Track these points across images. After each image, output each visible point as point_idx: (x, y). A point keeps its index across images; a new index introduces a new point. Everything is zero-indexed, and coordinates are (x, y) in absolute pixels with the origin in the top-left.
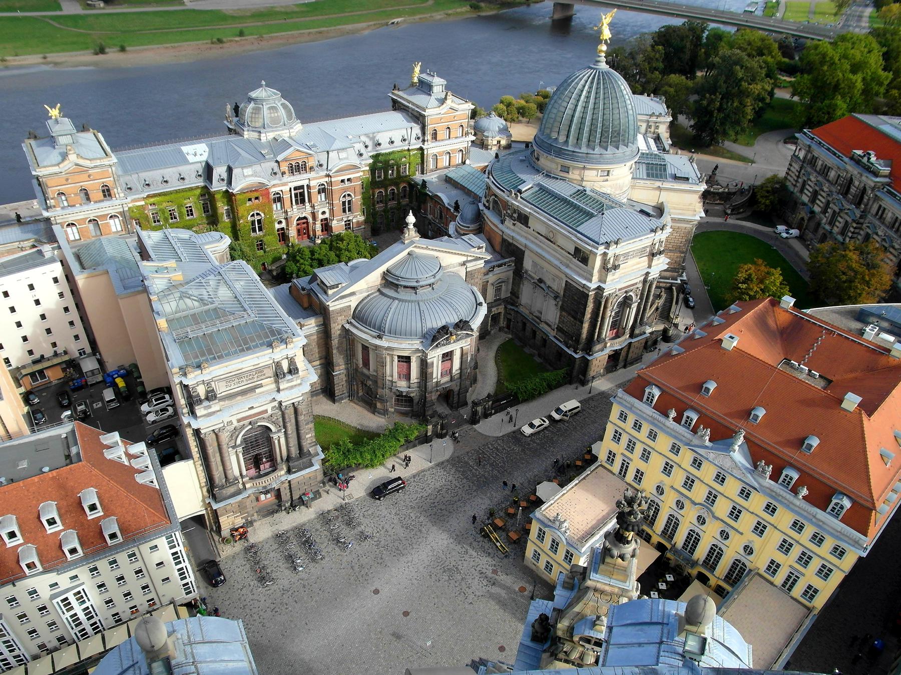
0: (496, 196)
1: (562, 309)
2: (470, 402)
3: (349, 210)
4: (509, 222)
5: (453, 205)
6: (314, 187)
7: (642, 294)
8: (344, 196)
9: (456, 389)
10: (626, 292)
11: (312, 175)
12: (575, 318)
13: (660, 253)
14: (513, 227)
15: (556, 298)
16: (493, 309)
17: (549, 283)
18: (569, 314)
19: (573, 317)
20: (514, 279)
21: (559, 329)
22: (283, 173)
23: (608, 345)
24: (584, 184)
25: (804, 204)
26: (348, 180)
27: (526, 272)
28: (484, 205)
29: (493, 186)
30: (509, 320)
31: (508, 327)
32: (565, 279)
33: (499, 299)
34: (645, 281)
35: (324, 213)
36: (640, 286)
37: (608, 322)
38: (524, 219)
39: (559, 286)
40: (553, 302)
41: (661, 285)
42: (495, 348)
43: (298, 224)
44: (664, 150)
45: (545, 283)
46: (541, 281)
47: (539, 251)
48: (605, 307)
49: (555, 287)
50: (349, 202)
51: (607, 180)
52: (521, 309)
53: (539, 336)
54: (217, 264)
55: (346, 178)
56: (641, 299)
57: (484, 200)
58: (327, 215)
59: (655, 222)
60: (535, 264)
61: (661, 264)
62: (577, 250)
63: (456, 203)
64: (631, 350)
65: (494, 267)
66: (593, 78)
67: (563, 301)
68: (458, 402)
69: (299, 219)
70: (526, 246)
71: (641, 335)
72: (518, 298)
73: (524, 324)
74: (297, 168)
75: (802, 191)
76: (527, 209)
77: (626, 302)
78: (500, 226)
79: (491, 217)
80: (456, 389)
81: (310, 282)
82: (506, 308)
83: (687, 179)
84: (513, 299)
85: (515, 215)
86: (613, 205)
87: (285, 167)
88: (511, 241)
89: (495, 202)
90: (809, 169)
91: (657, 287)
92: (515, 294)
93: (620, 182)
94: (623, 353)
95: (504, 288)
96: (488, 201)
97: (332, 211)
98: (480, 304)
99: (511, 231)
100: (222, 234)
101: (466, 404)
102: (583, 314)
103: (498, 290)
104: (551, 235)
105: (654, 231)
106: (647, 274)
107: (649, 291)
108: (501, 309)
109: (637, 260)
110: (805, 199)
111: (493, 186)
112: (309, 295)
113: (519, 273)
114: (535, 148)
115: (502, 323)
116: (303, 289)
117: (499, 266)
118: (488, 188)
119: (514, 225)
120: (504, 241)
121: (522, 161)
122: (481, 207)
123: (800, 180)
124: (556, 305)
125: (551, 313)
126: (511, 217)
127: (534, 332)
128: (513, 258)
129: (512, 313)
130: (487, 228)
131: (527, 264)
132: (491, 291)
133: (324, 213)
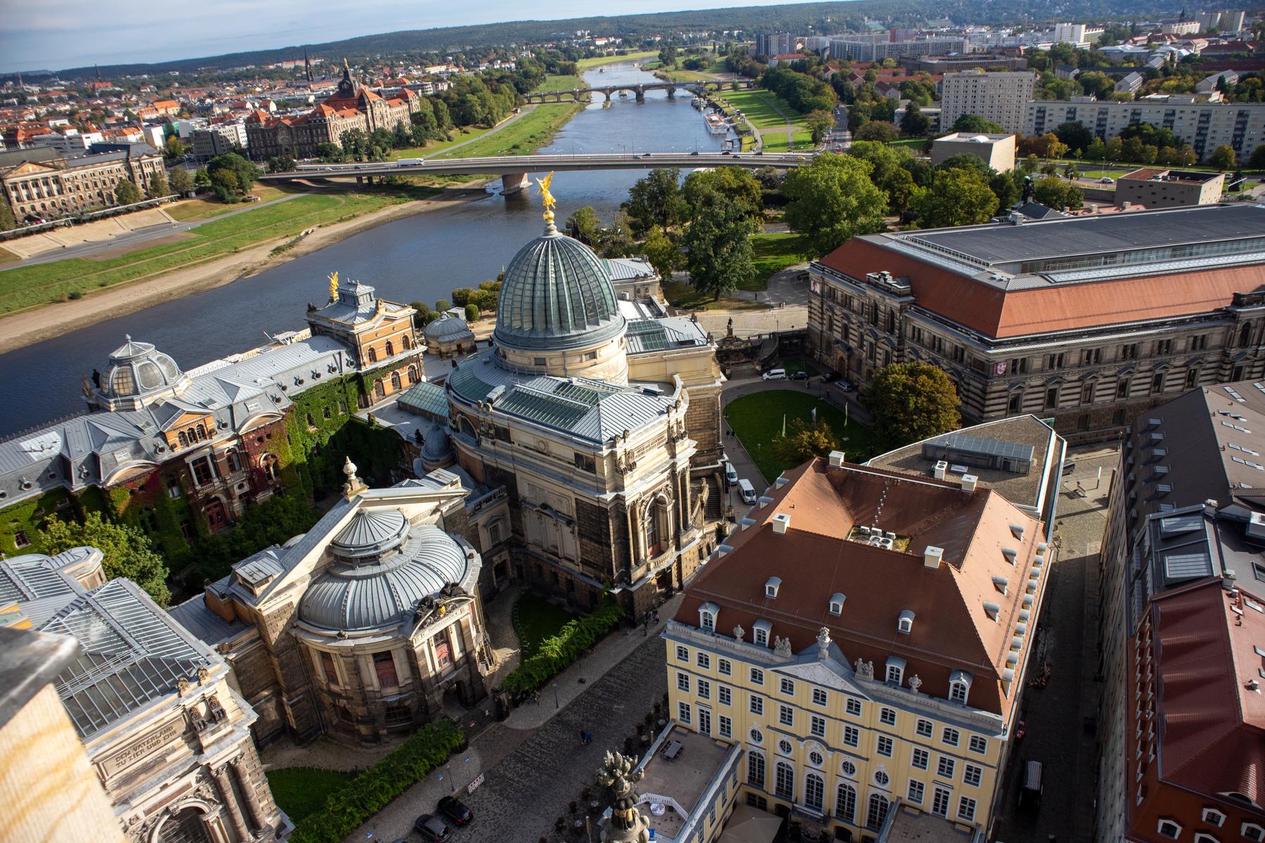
1: (581, 535)
2: (489, 691)
4: (486, 444)
7: (676, 491)
9: (466, 678)
10: (654, 494)
12: (600, 543)
13: (682, 436)
14: (492, 447)
15: (569, 522)
16: (495, 559)
17: (555, 507)
18: (591, 539)
19: (597, 542)
20: (511, 513)
21: (585, 562)
23: (652, 566)
25: (837, 342)
27: (524, 500)
29: (454, 402)
30: (519, 568)
31: (521, 576)
32: (574, 497)
33: (499, 544)
34: (673, 475)
37: (643, 537)
38: (503, 434)
39: (568, 508)
40: (567, 530)
42: (509, 609)
45: (551, 508)
46: (545, 506)
48: (634, 520)
49: (565, 511)
52: (532, 548)
53: (562, 577)
56: (676, 497)
59: (665, 401)
60: (532, 487)
61: (686, 449)
62: (578, 457)
64: (683, 566)
65: (480, 504)
66: (547, 250)
67: (579, 526)
68: (474, 696)
71: (690, 542)
72: (523, 535)
73: (540, 567)
75: (831, 329)
77: (656, 507)
80: (466, 678)
81: (230, 584)
82: (510, 552)
84: (516, 542)
85: (492, 432)
89: (464, 421)
91: (692, 480)
92: (518, 531)
94: (674, 572)
95: (500, 527)
96: (454, 422)
100: (90, 548)
101: (486, 694)
103: (494, 532)
104: (542, 446)
106: (674, 465)
107: (684, 486)
108: (505, 555)
109: (655, 451)
110: (838, 336)
111: (454, 402)
112: (232, 603)
113: (516, 504)
115: (512, 573)
116: (223, 596)
117: (487, 500)
118: (451, 405)
119: (494, 444)
120: (486, 467)
121: (486, 363)
122: (448, 431)
124: (573, 532)
125: (570, 544)
126: (487, 434)
127: (555, 574)
129: (521, 557)
130: (461, 456)
131: (524, 490)
132: (485, 537)
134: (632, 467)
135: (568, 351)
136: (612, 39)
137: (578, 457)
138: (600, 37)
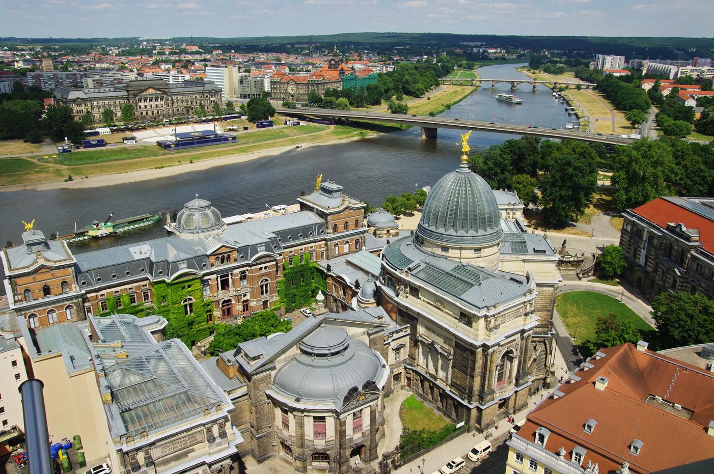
0: (390, 274)
5: (354, 284)
8: (262, 281)
26: (266, 268)
36: (519, 341)
41: (535, 339)
44: (522, 230)
54: (156, 342)
63: (357, 282)
70: (419, 314)
71: (524, 384)
77: (508, 356)
83: (544, 252)
88: (405, 310)
90: (637, 239)
98: (384, 366)
102: (473, 369)
123: (631, 248)
128: (408, 325)
138: (491, 47)
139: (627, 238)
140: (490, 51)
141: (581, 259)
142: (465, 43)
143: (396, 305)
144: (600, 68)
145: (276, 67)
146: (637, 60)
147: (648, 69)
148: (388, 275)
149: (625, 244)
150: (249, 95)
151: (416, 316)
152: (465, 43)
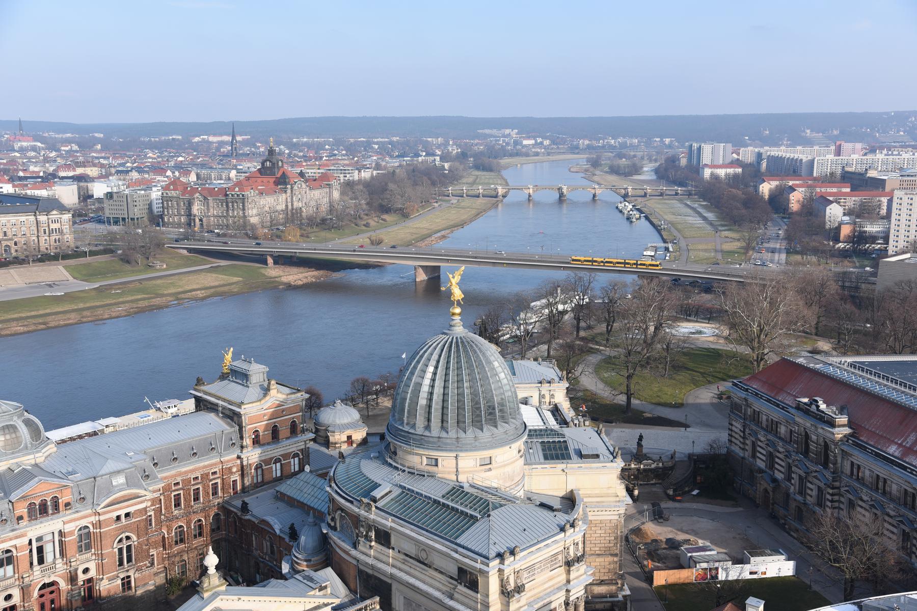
0: (342, 510)
3: (129, 560)
6: (71, 533)
8: (120, 541)
11: (68, 515)
13: (578, 559)
22: (20, 518)
24: (462, 478)
25: (761, 471)
26: (127, 515)
28: (329, 525)
35: (86, 571)
38: (384, 538)
43: (41, 596)
47: (412, 580)
50: (129, 547)
51: (490, 469)
55: (122, 513)
57: (329, 518)
58: (92, 573)
59: (562, 518)
69: (44, 586)
70: (392, 576)
74: (42, 510)
75: (754, 456)
76: (388, 523)
78: (353, 552)
79: (339, 542)
86: (503, 502)
87: (22, 510)
88: (370, 572)
90: (754, 428)
93: (508, 469)
96: (333, 519)
97: (101, 569)
99: (371, 555)
105: (563, 529)
114: (390, 439)
118: (332, 500)
123: (747, 442)
133: (86, 571)
134: (519, 589)
135: (461, 454)
136: (539, 140)
137: (461, 571)
138: (528, 138)
139: (739, 426)
140: (525, 142)
141: (670, 464)
142: (487, 131)
143: (355, 562)
144: (695, 162)
145: (173, 173)
146: (750, 148)
147: (768, 162)
148: (339, 512)
149: (737, 436)
150: (124, 219)
151: (389, 581)
152: (487, 131)
